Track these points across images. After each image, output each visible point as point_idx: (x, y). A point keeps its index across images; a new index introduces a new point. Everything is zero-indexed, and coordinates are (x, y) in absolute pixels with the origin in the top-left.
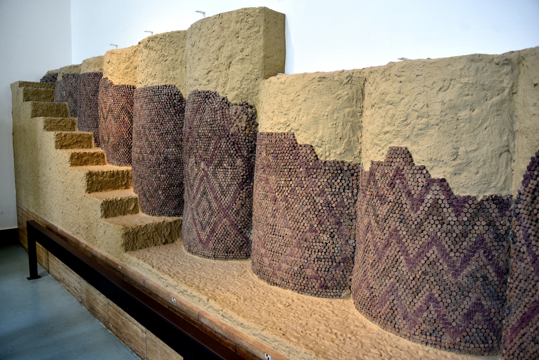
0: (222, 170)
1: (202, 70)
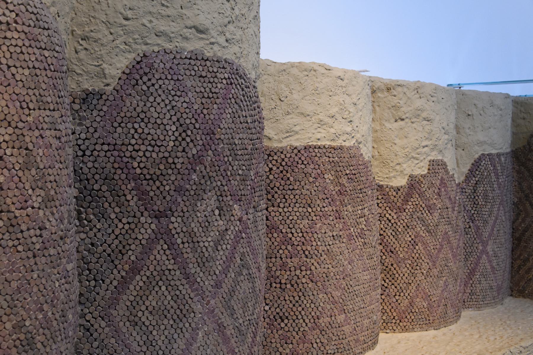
1: (216, 15)
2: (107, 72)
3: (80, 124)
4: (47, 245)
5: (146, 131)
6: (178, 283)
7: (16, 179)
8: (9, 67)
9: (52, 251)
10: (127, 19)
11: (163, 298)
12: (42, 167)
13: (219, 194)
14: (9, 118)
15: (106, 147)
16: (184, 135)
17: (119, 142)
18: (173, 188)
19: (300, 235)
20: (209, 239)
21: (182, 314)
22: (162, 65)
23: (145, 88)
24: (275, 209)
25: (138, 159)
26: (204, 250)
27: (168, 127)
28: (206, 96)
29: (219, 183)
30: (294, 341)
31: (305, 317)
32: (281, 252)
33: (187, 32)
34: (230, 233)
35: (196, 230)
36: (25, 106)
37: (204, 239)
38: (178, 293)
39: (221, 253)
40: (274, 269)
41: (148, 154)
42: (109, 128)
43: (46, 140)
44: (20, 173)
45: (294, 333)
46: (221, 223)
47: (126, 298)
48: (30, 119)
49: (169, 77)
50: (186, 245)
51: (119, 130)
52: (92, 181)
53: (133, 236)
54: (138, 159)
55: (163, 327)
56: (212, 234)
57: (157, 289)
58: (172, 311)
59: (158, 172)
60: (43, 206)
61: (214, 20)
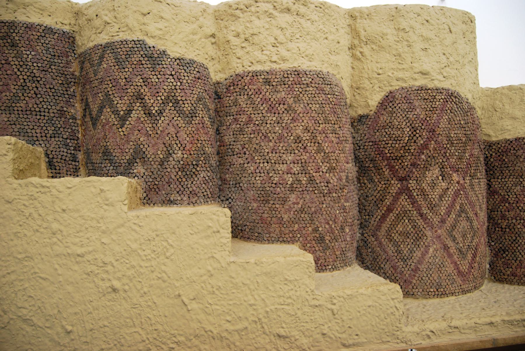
0: (477, 181)
2: (370, 104)
3: (357, 133)
4: (332, 191)
5: (392, 133)
6: (416, 218)
7: (313, 158)
8: (308, 104)
9: (334, 195)
10: (379, 74)
11: (406, 226)
12: (327, 151)
13: (441, 166)
14: (308, 128)
15: (371, 144)
16: (414, 133)
17: (377, 140)
18: (409, 164)
19: (515, 196)
20: (435, 193)
21: (419, 237)
22: (400, 96)
23: (390, 109)
24: (496, 180)
25: (388, 148)
26: (432, 200)
27: (404, 130)
28: (428, 109)
29: (441, 161)
30: (513, 267)
31: (521, 251)
32: (501, 207)
33: (416, 76)
34: (450, 190)
35: (426, 188)
36: (317, 122)
37: (432, 193)
38: (415, 224)
39: (445, 202)
40: (497, 218)
41: (393, 145)
42: (372, 133)
43: (329, 139)
44: (315, 155)
45: (513, 261)
46: (443, 184)
47: (385, 227)
48: (320, 129)
49: (405, 102)
50: (420, 197)
51: (378, 134)
52: (365, 162)
53: (388, 191)
54: (388, 148)
55: (407, 243)
56: (437, 190)
57: (402, 221)
58: (412, 235)
59: (400, 155)
60: (328, 171)
61: (434, 67)
